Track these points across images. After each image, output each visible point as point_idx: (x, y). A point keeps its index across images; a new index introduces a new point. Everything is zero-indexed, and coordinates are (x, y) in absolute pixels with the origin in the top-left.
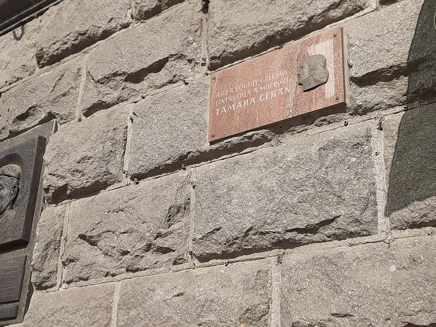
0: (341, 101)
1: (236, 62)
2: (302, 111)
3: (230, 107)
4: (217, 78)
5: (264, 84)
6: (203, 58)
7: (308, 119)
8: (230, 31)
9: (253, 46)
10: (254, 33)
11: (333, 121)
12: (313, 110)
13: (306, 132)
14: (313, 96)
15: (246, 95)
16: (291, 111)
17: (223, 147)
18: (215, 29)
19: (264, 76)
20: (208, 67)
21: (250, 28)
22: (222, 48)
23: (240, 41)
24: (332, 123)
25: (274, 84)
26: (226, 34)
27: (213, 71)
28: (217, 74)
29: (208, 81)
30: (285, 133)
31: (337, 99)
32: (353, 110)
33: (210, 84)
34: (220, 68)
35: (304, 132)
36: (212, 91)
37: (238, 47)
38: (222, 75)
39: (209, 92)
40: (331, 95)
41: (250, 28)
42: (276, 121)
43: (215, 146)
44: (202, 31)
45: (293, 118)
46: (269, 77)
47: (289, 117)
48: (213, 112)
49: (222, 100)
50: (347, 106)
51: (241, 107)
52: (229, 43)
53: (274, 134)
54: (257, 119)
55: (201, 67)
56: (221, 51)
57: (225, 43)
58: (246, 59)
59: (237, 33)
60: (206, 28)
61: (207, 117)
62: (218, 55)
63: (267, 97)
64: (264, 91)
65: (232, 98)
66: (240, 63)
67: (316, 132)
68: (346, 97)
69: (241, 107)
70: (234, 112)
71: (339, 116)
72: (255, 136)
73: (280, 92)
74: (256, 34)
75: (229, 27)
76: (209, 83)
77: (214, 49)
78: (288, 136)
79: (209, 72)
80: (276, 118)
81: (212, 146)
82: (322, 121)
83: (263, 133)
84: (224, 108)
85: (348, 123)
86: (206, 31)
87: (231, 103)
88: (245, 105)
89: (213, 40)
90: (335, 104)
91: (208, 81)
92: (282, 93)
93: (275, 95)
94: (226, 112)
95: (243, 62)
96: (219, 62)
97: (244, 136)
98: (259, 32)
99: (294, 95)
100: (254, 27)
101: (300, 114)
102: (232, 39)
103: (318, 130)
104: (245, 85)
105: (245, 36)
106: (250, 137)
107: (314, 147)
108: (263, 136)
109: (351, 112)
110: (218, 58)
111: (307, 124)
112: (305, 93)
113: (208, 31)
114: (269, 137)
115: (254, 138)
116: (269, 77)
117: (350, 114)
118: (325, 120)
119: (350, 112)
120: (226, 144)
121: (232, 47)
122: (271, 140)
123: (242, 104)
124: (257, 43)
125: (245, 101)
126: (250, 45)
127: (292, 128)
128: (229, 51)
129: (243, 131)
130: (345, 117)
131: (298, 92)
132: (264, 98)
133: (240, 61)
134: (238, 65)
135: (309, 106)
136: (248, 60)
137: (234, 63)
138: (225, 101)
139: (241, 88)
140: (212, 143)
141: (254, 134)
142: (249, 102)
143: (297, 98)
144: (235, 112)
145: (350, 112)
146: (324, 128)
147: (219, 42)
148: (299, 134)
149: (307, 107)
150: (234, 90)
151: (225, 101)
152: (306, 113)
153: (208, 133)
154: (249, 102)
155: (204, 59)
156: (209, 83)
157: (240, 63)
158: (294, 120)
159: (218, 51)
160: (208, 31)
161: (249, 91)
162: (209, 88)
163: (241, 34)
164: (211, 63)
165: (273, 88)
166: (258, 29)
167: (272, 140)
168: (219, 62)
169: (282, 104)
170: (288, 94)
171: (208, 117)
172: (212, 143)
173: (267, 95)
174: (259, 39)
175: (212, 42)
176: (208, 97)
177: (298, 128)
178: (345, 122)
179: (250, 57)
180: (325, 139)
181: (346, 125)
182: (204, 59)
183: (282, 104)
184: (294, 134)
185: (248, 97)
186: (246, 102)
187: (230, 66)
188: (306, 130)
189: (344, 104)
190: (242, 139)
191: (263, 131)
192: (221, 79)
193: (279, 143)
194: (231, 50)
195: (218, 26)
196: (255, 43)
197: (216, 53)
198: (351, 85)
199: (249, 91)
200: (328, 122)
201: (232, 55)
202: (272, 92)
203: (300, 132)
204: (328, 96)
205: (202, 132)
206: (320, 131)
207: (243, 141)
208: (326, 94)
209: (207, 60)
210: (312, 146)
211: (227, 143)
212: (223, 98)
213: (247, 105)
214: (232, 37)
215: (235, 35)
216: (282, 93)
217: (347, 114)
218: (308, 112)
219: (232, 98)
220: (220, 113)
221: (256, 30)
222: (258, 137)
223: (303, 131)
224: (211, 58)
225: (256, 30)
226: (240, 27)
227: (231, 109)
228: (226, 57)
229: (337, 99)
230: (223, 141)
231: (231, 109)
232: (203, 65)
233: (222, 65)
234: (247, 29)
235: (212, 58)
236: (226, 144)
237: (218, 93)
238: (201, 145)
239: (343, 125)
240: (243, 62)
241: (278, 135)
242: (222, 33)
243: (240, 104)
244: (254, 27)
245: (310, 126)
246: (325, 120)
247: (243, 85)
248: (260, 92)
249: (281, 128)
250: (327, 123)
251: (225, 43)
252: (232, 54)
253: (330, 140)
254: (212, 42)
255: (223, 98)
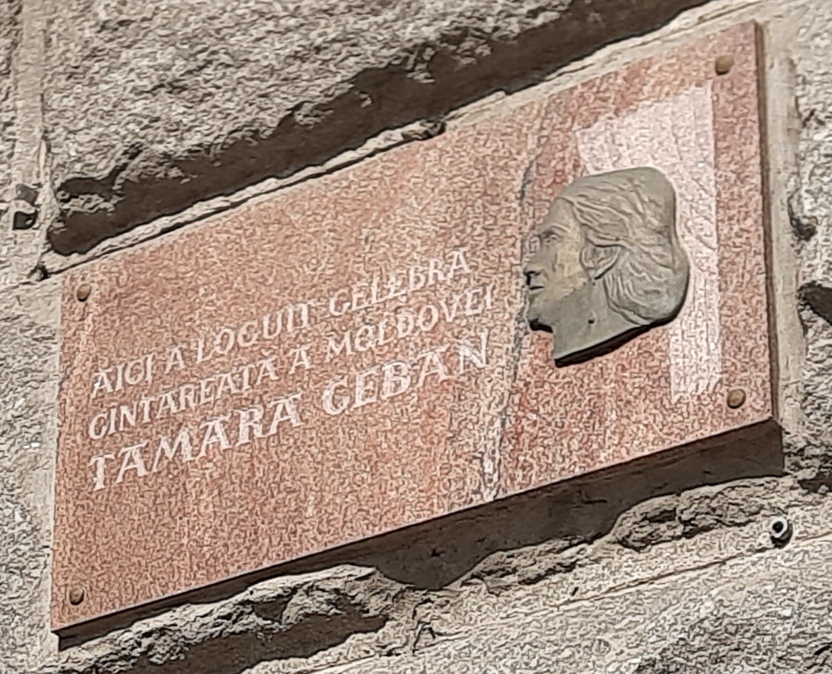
0: (754, 412)
1: (198, 209)
2: (549, 468)
3: (164, 445)
4: (95, 295)
5: (344, 326)
6: (23, 188)
7: (576, 510)
8: (168, 41)
9: (287, 122)
10: (295, 56)
11: (710, 520)
12: (605, 459)
13: (570, 576)
14: (607, 388)
15: (252, 383)
16: (489, 466)
17: (127, 658)
18: (88, 34)
19: (344, 280)
20: (49, 236)
21: (270, 25)
22: (122, 132)
23: (218, 98)
24: (707, 529)
25: (400, 327)
26: (146, 60)
27: (75, 258)
28: (98, 269)
29: (47, 306)
30: (455, 586)
31: (735, 404)
32: (817, 462)
33: (57, 326)
34: (115, 241)
35: (555, 578)
36: (68, 360)
37: (207, 129)
38: (123, 278)
39: (54, 365)
40: (703, 384)
41: (270, 25)
42: (408, 519)
43: (85, 655)
44: (15, 44)
45: (499, 505)
46: (374, 290)
47: (477, 501)
48: (75, 473)
49: (124, 410)
50: (786, 439)
51: (224, 445)
52: (158, 108)
53: (398, 587)
54: (310, 511)
55: (11, 233)
56: (120, 148)
57: (139, 107)
58: (252, 190)
59: (205, 52)
60: (39, 25)
61: (44, 498)
62: (102, 168)
63: (359, 392)
64: (345, 363)
65: (176, 399)
66: (219, 210)
67: (621, 578)
68: (782, 394)
69: (224, 445)
70: (185, 472)
71: (745, 492)
72: (296, 599)
73: (432, 365)
74: (303, 60)
75: (158, 20)
76: (54, 321)
77: (81, 137)
78: (471, 597)
79: (53, 261)
80: (411, 502)
81: (73, 652)
82: (652, 520)
83: (339, 584)
84: (134, 450)
85: (789, 532)
86: (39, 42)
87: (173, 424)
88: (244, 438)
89: (78, 89)
90: (722, 429)
91: (47, 306)
92: (441, 371)
93: (405, 383)
94: (142, 472)
95: (234, 205)
96: (109, 205)
97: (240, 597)
98: (318, 49)
99: (507, 384)
100: (292, 22)
101: (537, 480)
102: (175, 88)
103: (632, 566)
104: (243, 331)
105: (244, 72)
106: (273, 608)
107: (610, 656)
108: (340, 598)
109: (807, 474)
110: (104, 187)
111: (573, 537)
112: (563, 371)
113: (48, 42)
114: (375, 605)
115: (291, 613)
116: (374, 290)
117: (802, 483)
118: (667, 516)
119: (801, 475)
120: (146, 642)
121: (176, 129)
122: (382, 620)
123: (231, 428)
124: (307, 107)
125: (244, 415)
126: (271, 120)
127: (496, 556)
128: (161, 148)
129: (235, 572)
130: (775, 500)
131: (524, 369)
132: (346, 401)
133: (218, 202)
134: (208, 226)
135: (585, 444)
136: (263, 196)
137: (187, 215)
138: (139, 415)
139: (223, 346)
140: (69, 637)
141: (294, 590)
142: (268, 418)
143: (521, 397)
144: (193, 472)
145: (801, 475)
146: (665, 556)
147: (107, 100)
148: (530, 588)
149: (575, 444)
150: (188, 355)
151: (139, 415)
152: (567, 475)
153: (47, 584)
154: (268, 418)
155: (29, 194)
156: (54, 321)
157: (219, 210)
158: (504, 514)
159: (102, 151)
160: (48, 42)
161: (267, 364)
162: (55, 348)
163: (225, 59)
164: (63, 213)
165: (395, 348)
166: (313, 35)
167: (387, 619)
168: (109, 205)
169: (439, 429)
170: (474, 375)
171: (51, 500)
172: (69, 637)
173: (360, 383)
174: (319, 85)
175: (69, 102)
176: (49, 393)
177: (527, 560)
178: (778, 527)
179: (272, 183)
180: (668, 615)
181: (779, 543)
182: (29, 194)
183: (439, 429)
184: (507, 587)
185: (260, 394)
186: (249, 422)
187: (165, 231)
188: (570, 568)
189: (771, 430)
190: (228, 617)
191: (340, 576)
192: (120, 299)
193: (426, 637)
194: (171, 145)
195: (103, 16)
196: (298, 107)
197: (91, 159)
198: (806, 329)
199: (267, 364)
200: (686, 523)
201: (174, 173)
202: (388, 368)
203: (539, 578)
204: (683, 388)
205: (17, 581)
206: (645, 575)
207: (237, 628)
208: (674, 380)
209: (46, 198)
210: (602, 654)
211: (147, 635)
212: (128, 397)
213: (258, 434)
214: (176, 72)
215: (192, 66)
216: (441, 370)
217: (788, 481)
218: (578, 472)
219: (176, 399)
220: (110, 476)
221: (306, 37)
222: (314, 604)
223: (552, 571)
224: (63, 186)
225: (306, 37)
226: (217, 24)
227: (170, 454)
228: (146, 182)
229: (735, 404)
230: (127, 627)
231: (170, 454)
232: (23, 221)
233: (122, 225)
234: (255, 33)
235: (73, 188)
236: (146, 642)
237: (103, 374)
238: (14, 649)
239: (765, 541)
240: (234, 205)
241: (419, 595)
242: (125, 55)
243: (219, 430)
244: (292, 22)
245: (589, 549)
246: (667, 516)
247: (236, 329)
248: (324, 369)
249: (433, 556)
250: (679, 531)
251: (139, 107)
252: (177, 163)
253: (693, 618)
254: (69, 102)
255: (128, 397)
